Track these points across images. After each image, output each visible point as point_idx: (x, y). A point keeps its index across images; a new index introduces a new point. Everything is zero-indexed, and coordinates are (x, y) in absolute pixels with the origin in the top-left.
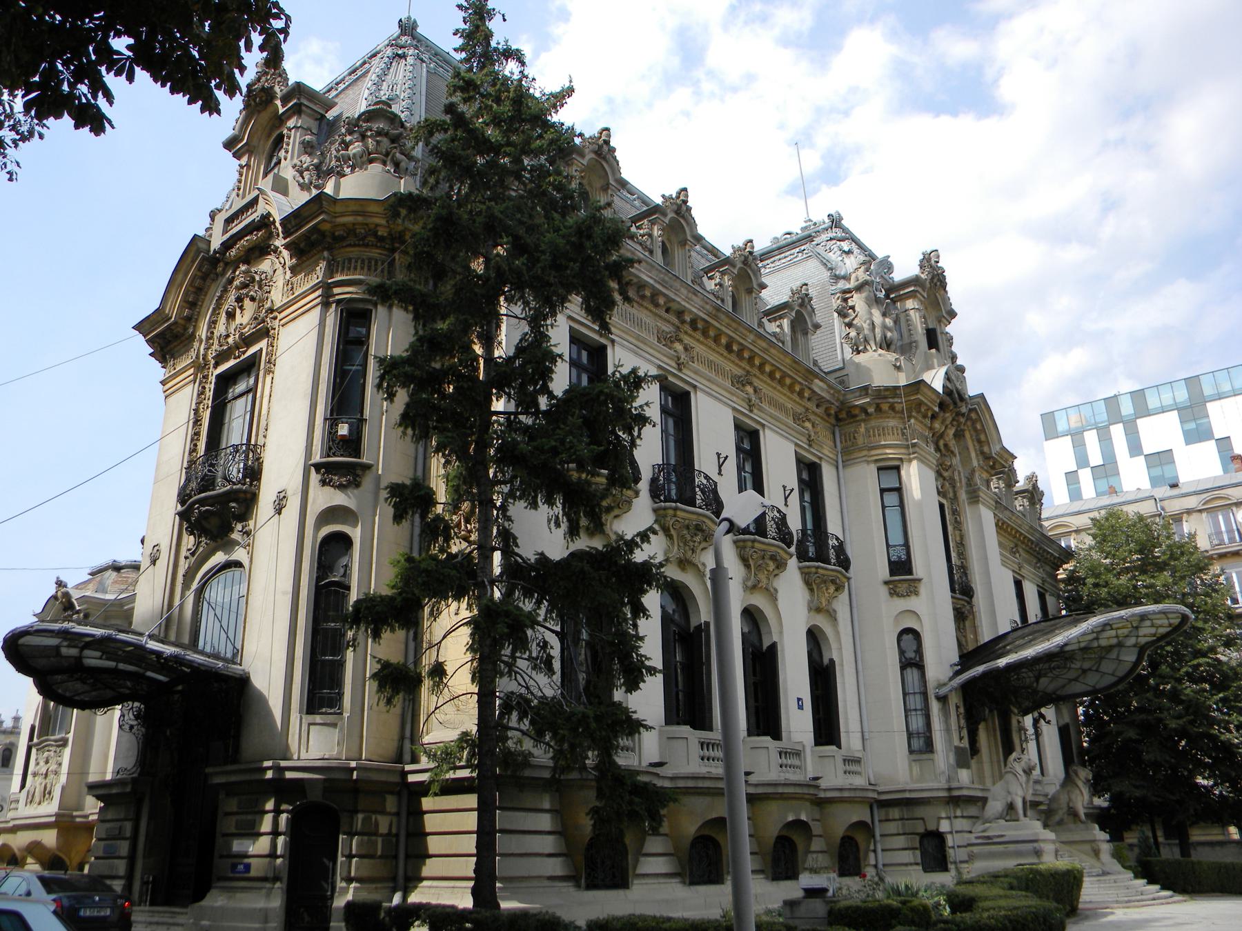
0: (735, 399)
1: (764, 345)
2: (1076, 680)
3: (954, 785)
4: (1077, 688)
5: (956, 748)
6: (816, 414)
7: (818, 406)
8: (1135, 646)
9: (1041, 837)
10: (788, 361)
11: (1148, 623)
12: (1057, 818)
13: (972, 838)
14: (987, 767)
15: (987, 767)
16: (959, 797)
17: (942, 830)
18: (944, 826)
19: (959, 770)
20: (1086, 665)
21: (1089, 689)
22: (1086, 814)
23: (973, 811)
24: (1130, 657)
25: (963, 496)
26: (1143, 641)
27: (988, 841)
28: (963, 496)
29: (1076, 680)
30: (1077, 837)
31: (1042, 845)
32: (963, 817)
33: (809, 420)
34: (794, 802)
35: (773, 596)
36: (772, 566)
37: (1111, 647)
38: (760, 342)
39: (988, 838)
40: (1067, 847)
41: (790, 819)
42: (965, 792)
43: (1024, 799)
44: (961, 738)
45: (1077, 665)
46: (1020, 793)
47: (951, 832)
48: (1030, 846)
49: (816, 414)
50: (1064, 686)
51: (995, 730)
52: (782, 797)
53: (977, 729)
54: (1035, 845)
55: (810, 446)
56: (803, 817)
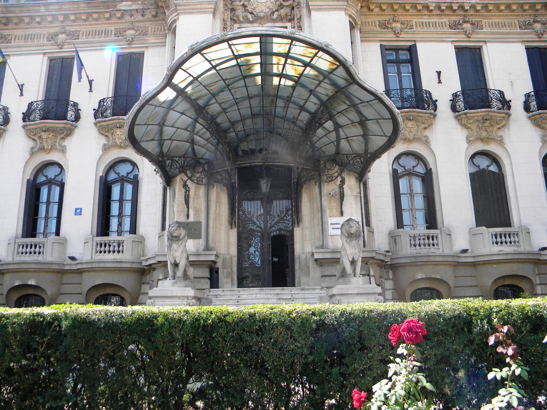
0: (44, 48)
1: (56, 7)
6: (141, 21)
7: (143, 16)
10: (82, 5)
14: (307, 232)
15: (307, 232)
21: (385, 139)
25: (304, 11)
28: (304, 11)
33: (129, 29)
34: (22, 274)
35: (63, 150)
36: (44, 135)
38: (50, 7)
41: (17, 284)
49: (141, 21)
52: (9, 271)
55: (129, 44)
56: (32, 282)
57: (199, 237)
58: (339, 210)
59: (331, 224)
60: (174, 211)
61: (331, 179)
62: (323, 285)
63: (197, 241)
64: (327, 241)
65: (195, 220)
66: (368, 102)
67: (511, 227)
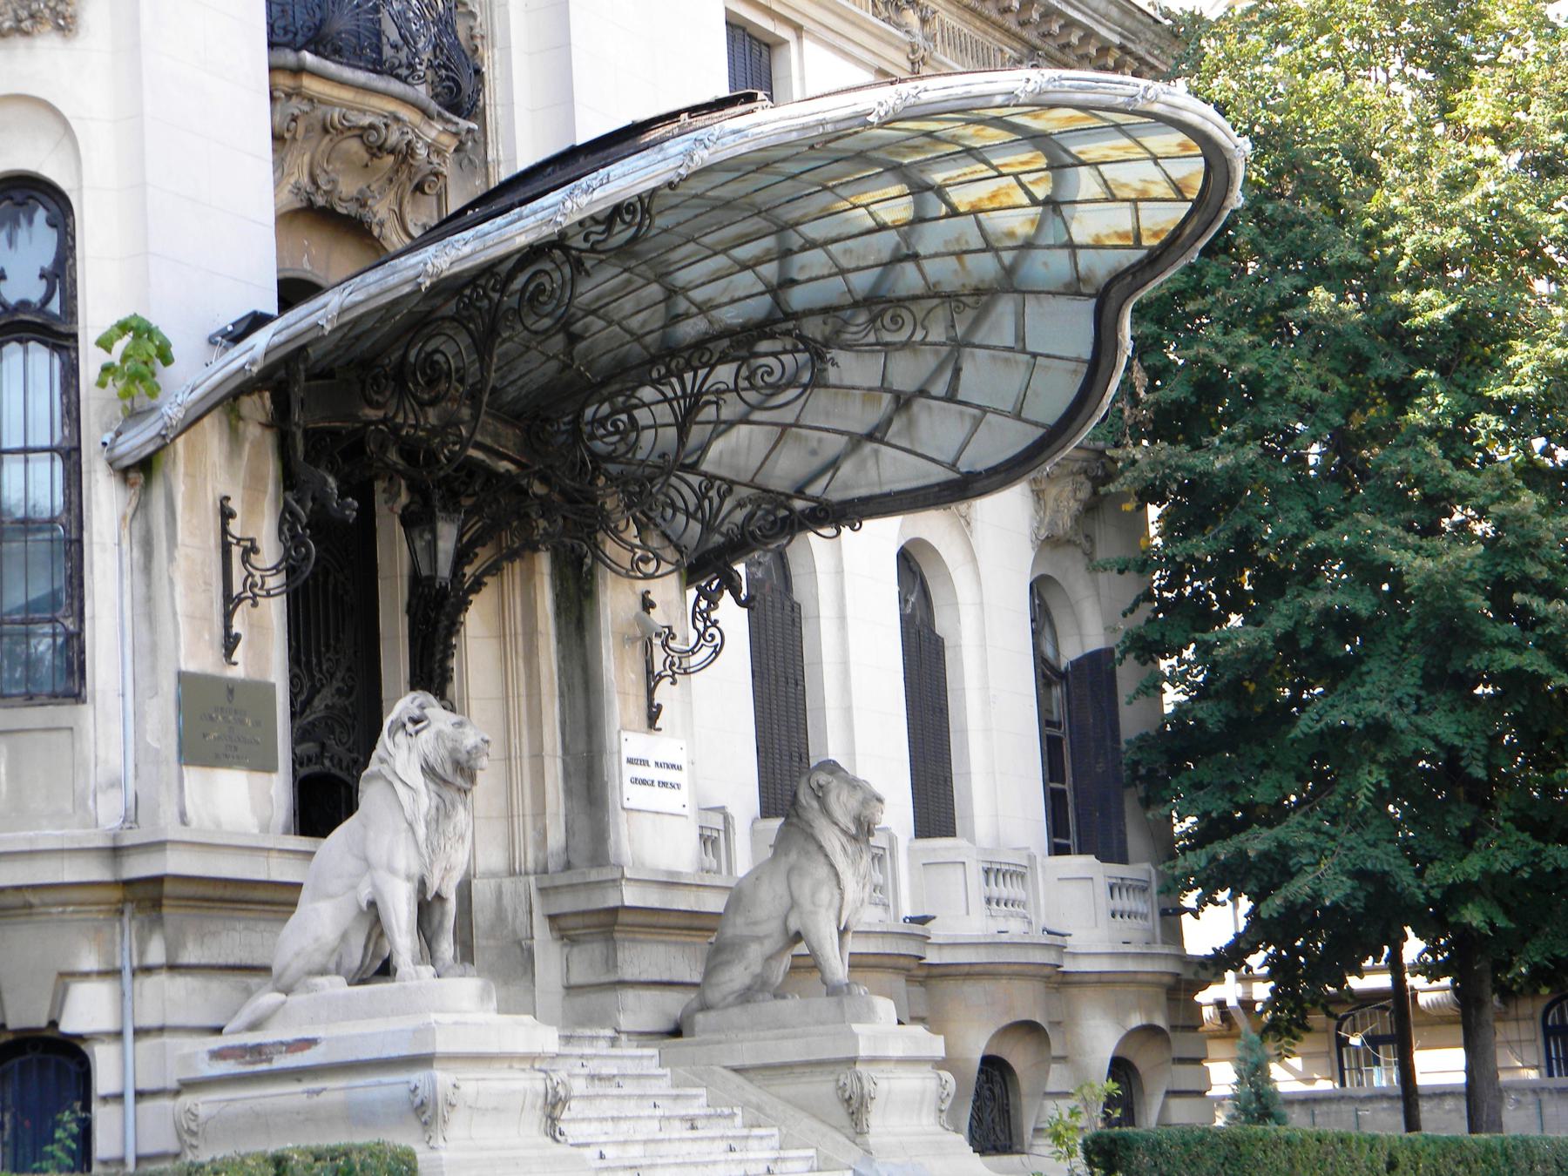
2: (875, 435)
3: (129, 839)
4: (892, 469)
5: (183, 678)
8: (1074, 288)
9: (441, 1047)
11: (1086, 183)
12: (737, 976)
13: (195, 1055)
16: (158, 880)
17: (68, 1026)
18: (88, 1010)
19: (193, 775)
20: (906, 372)
21: (939, 475)
22: (858, 963)
23: (235, 940)
24: (1065, 330)
26: (1100, 266)
27: (255, 1065)
29: (875, 435)
30: (791, 1051)
31: (442, 1077)
32: (173, 968)
37: (983, 296)
39: (257, 1051)
40: (751, 1092)
42: (176, 863)
43: (422, 885)
44: (230, 642)
45: (849, 368)
46: (405, 859)
47: (118, 1035)
48: (394, 1084)
50: (833, 465)
51: (531, 632)
53: (454, 627)
54: (417, 1077)
57: (269, 767)
58: (643, 702)
59: (630, 761)
60: (175, 614)
61: (632, 572)
62: (626, 1022)
63: (260, 778)
64: (618, 833)
65: (257, 677)
66: (1035, 355)
67: (951, 832)
